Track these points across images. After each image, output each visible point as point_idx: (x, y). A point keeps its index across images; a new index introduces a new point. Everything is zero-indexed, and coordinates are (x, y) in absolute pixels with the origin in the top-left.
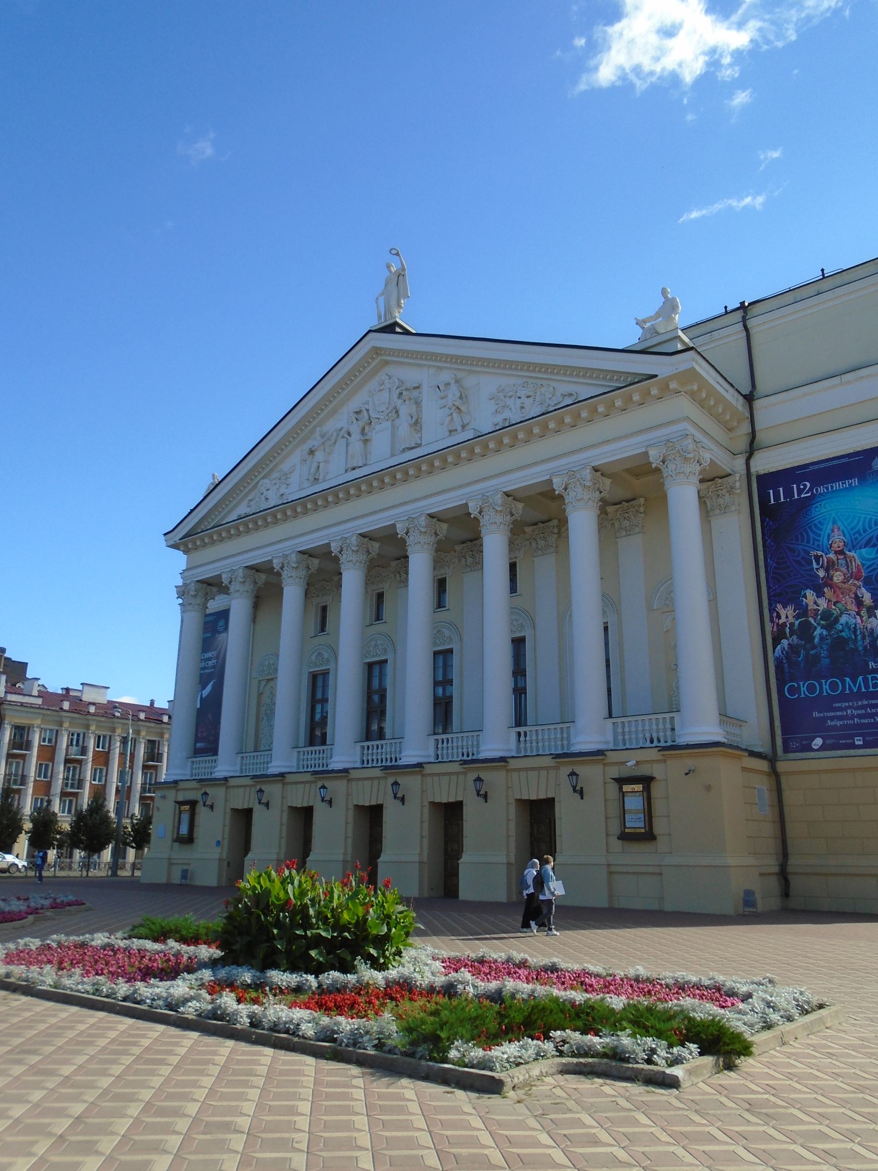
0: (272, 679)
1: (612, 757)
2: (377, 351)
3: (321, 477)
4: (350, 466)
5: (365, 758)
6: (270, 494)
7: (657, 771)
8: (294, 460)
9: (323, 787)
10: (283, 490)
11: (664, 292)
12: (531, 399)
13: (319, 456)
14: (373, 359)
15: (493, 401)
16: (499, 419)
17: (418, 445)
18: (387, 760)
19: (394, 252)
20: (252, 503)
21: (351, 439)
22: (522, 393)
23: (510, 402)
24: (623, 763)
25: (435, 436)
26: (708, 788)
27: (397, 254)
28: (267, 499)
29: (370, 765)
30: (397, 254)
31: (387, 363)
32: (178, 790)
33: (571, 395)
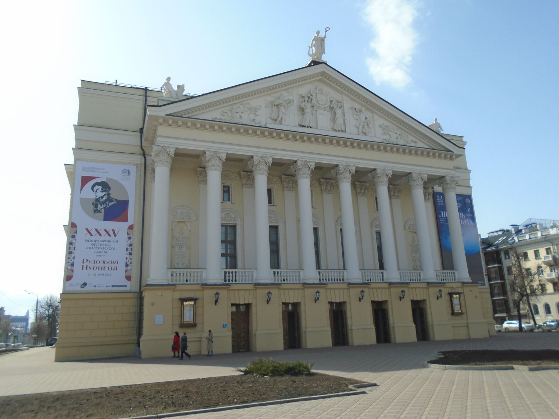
0: (184, 222)
1: (448, 285)
2: (323, 74)
3: (283, 121)
4: (307, 124)
5: (321, 278)
6: (243, 115)
7: (460, 290)
8: (260, 102)
9: (318, 292)
10: (252, 116)
11: (436, 119)
12: (399, 137)
13: (282, 109)
14: (318, 76)
15: (381, 129)
16: (387, 137)
17: (345, 131)
18: (332, 279)
19: (328, 29)
20: (225, 114)
21: (306, 111)
22: (398, 133)
23: (390, 133)
24: (453, 288)
25: (352, 132)
26: (476, 297)
27: (326, 31)
28: (241, 117)
29: (336, 281)
30: (326, 31)
31: (319, 81)
32: (173, 291)
33: (416, 142)
